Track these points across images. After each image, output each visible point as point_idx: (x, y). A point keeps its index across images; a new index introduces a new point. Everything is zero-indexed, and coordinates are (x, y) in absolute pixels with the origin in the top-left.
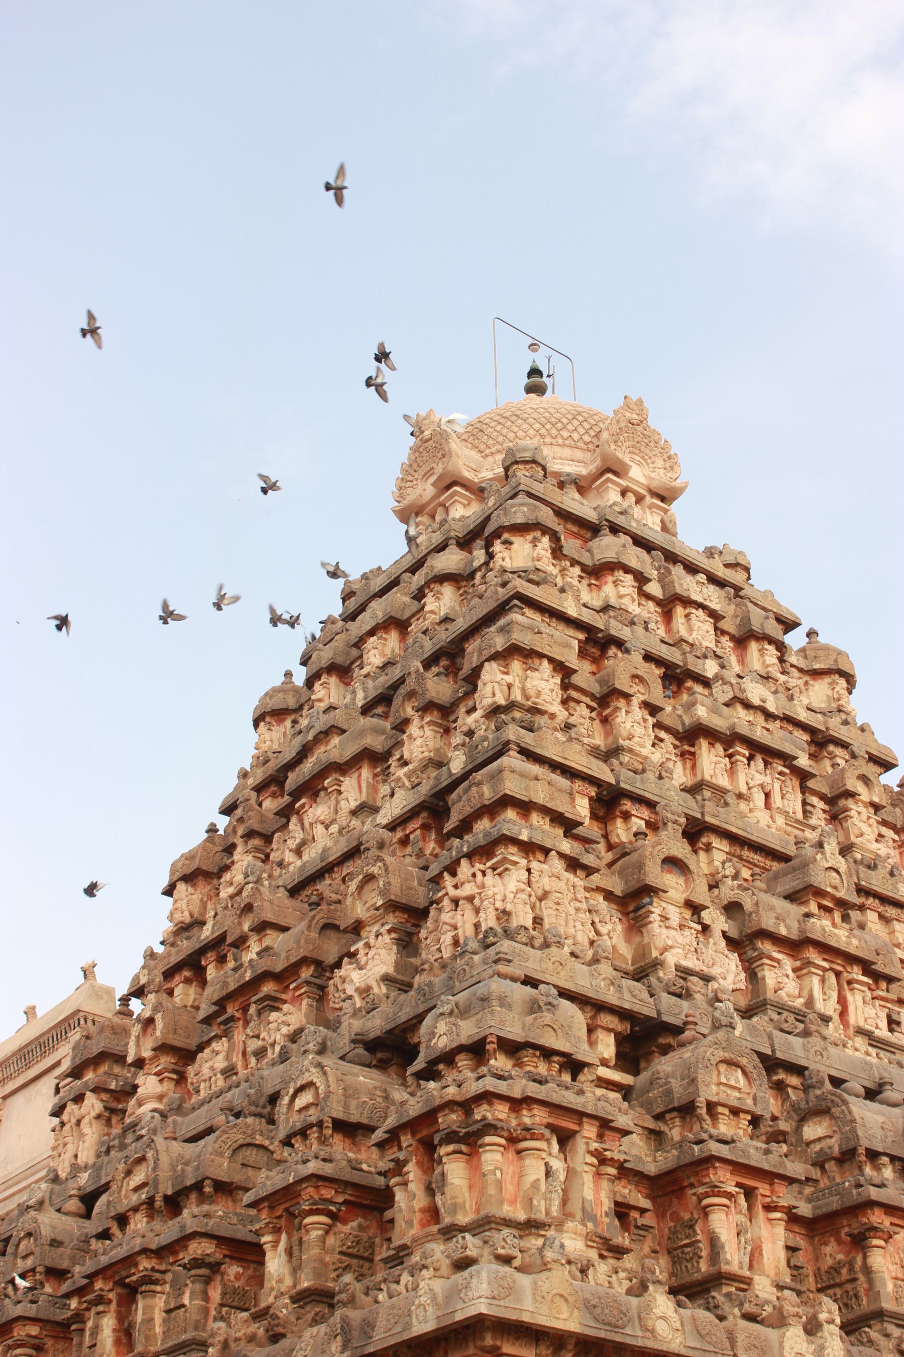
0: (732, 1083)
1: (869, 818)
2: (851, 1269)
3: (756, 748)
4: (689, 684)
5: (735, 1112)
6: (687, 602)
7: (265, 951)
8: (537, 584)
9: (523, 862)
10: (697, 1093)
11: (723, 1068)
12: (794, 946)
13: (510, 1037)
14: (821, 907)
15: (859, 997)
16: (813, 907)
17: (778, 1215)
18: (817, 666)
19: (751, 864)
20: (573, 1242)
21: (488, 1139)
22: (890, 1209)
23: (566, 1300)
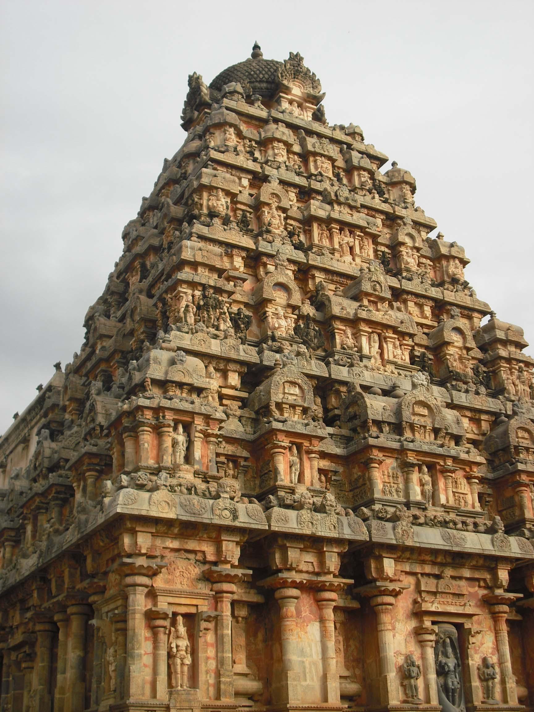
0: (292, 392)
1: (413, 255)
2: (364, 479)
3: (344, 225)
4: (314, 195)
5: (293, 406)
6: (315, 154)
7: (103, 348)
8: (223, 152)
9: (190, 292)
11: (287, 385)
12: (354, 322)
13: (158, 378)
14: (369, 301)
15: (390, 346)
16: (366, 302)
17: (313, 455)
19: (341, 284)
20: (187, 475)
21: (141, 428)
22: (382, 449)
23: (168, 504)
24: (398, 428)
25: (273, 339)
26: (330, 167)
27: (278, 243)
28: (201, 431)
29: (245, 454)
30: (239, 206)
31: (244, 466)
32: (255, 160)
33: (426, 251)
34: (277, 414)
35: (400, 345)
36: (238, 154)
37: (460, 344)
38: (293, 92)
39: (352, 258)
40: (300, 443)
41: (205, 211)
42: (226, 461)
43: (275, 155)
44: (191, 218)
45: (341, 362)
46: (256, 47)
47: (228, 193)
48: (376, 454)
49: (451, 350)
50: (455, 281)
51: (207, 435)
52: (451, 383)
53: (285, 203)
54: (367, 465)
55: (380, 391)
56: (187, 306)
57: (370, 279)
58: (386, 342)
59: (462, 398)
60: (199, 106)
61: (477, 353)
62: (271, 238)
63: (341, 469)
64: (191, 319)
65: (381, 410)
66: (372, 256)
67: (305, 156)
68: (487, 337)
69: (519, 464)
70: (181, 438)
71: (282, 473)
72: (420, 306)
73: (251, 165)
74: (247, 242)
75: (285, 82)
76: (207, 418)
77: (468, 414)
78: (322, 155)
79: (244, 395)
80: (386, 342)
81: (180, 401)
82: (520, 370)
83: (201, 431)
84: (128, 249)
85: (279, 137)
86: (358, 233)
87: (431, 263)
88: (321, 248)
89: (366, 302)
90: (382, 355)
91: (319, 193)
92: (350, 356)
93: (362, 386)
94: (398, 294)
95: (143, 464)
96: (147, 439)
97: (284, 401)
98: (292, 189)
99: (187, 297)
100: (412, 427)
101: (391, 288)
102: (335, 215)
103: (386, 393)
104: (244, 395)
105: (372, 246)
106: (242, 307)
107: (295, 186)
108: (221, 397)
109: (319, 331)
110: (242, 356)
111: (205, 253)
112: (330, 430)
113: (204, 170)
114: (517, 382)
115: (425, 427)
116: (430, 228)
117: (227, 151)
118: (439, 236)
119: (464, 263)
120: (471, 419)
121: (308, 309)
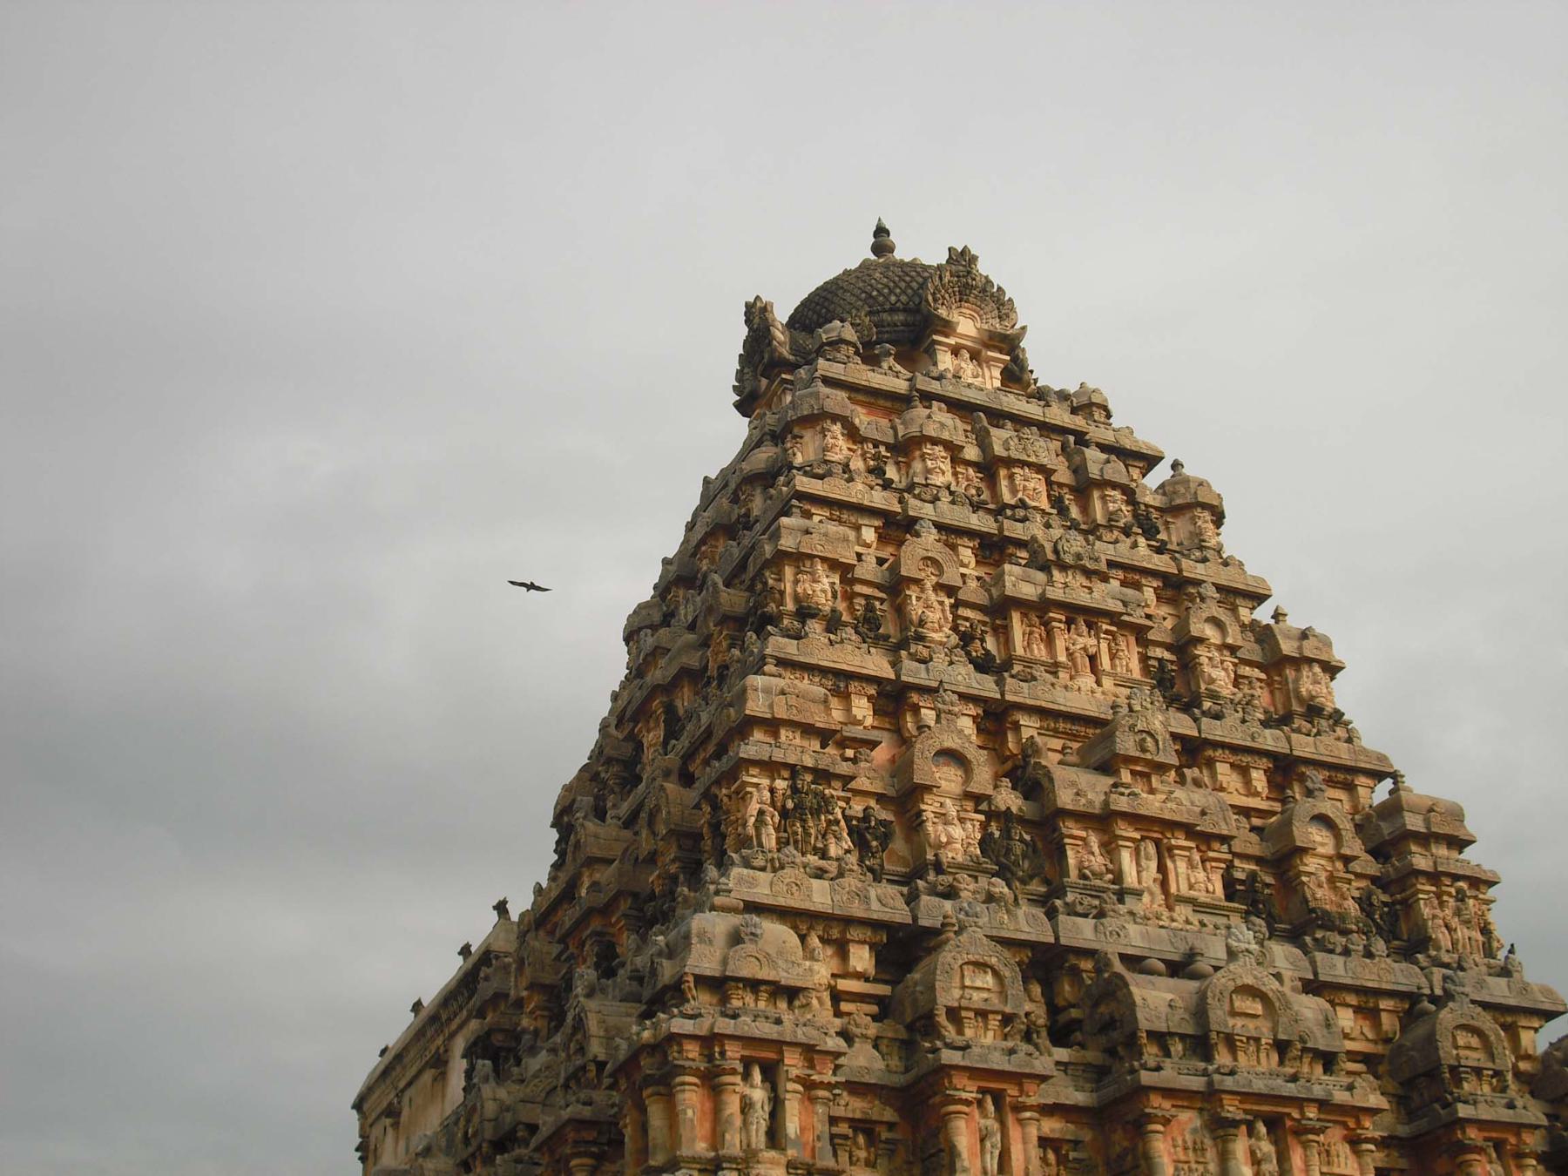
0: (979, 984)
1: (1222, 662)
3: (1077, 614)
4: (1011, 550)
5: (982, 1014)
6: (1009, 463)
7: (595, 886)
8: (821, 477)
9: (765, 782)
10: (934, 1001)
11: (968, 970)
12: (1103, 821)
13: (708, 973)
14: (1133, 773)
15: (1182, 866)
16: (1126, 776)
17: (1028, 1114)
18: (1179, 501)
19: (1074, 737)
22: (1168, 1093)
24: (1201, 1045)
25: (939, 868)
26: (1042, 488)
27: (940, 660)
28: (798, 1079)
29: (889, 1115)
30: (858, 588)
31: (887, 1141)
32: (887, 485)
33: (1251, 650)
34: (950, 1032)
35: (1203, 861)
36: (850, 480)
37: (1329, 849)
38: (960, 330)
39: (1094, 679)
40: (1000, 1091)
41: (790, 606)
42: (850, 1132)
43: (928, 471)
44: (763, 622)
45: (1079, 909)
46: (881, 231)
47: (833, 565)
48: (1158, 1105)
49: (1311, 864)
50: (1313, 711)
51: (809, 1085)
52: (1312, 935)
53: (951, 577)
54: (1139, 1127)
55: (1161, 966)
56: (761, 813)
57: (1132, 727)
58: (1172, 857)
59: (1336, 968)
60: (770, 365)
61: (1367, 865)
62: (925, 653)
63: (1087, 1135)
64: (770, 838)
65: (1164, 1009)
66: (1137, 674)
67: (989, 468)
68: (1386, 829)
69: (1460, 1106)
70: (759, 1094)
71: (965, 1154)
72: (1243, 771)
73: (879, 499)
74: (877, 664)
75: (942, 312)
76: (810, 1052)
77: (1352, 999)
78: (1023, 464)
79: (882, 990)
80: (1172, 857)
81: (755, 1018)
82: (1461, 897)
83: (798, 1079)
84: (636, 671)
85: (933, 434)
86: (1105, 627)
87: (1263, 676)
88: (1029, 663)
89: (1126, 776)
90: (1164, 884)
91: (1020, 544)
92: (1097, 893)
93: (1126, 959)
94: (1193, 751)
95: (685, 1152)
96: (691, 1099)
97: (964, 1003)
98: (966, 541)
99: (760, 795)
100: (1230, 1041)
101: (1175, 737)
102: (1056, 593)
103: (1179, 968)
104: (882, 990)
105: (1135, 649)
106: (872, 803)
107: (970, 533)
108: (837, 997)
109: (1030, 844)
110: (877, 911)
111: (792, 700)
112: (1062, 1054)
113: (784, 520)
114: (1455, 922)
115: (1257, 1040)
116: (1259, 598)
117: (829, 474)
118: (1278, 616)
119: (1332, 670)
120: (1358, 1010)
121: (1008, 799)
